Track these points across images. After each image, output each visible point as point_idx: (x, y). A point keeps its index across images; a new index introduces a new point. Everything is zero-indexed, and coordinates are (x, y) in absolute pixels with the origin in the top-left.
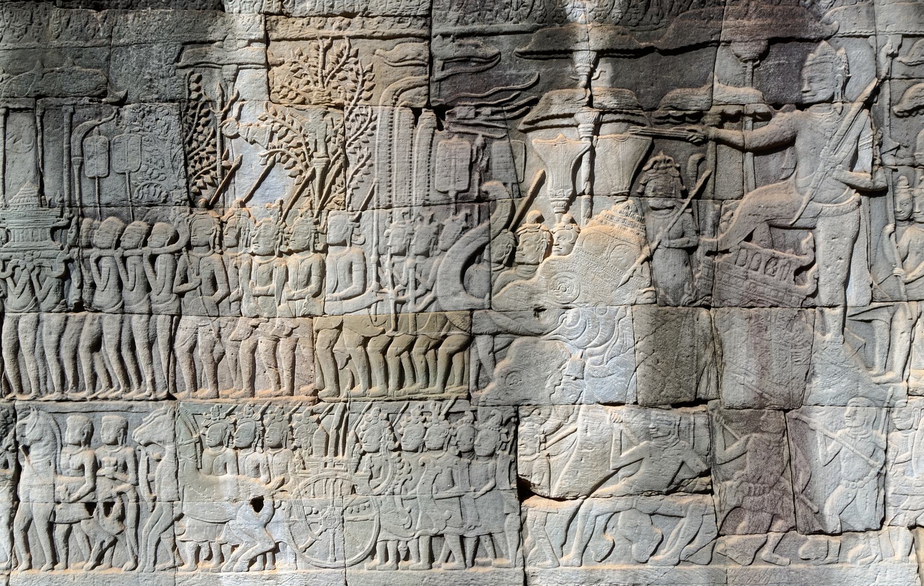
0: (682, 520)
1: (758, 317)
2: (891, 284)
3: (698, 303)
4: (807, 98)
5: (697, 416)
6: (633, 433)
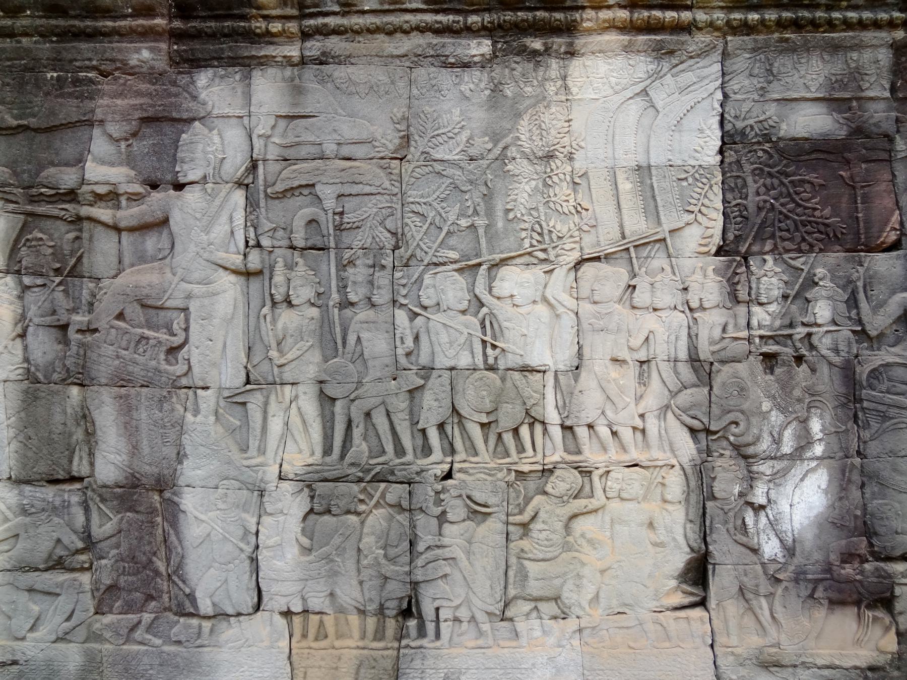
0: (60, 598)
1: (127, 396)
2: (265, 367)
3: (69, 381)
4: (182, 180)
5: (71, 494)
6: (9, 508)
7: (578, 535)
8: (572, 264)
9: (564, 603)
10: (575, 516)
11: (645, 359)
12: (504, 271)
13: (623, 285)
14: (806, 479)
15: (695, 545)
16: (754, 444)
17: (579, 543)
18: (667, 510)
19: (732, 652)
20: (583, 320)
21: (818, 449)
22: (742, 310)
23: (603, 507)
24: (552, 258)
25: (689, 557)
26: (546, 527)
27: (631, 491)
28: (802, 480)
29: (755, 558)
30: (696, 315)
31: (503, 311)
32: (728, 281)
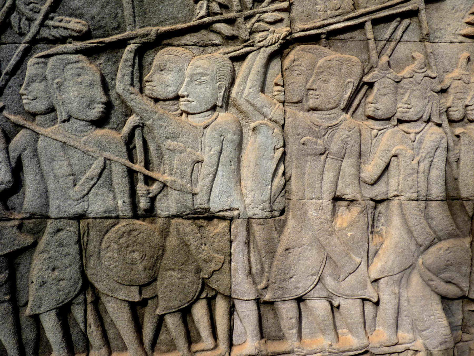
8: (275, 47)
11: (384, 197)
12: (162, 56)
13: (353, 81)
24: (244, 34)
31: (164, 122)
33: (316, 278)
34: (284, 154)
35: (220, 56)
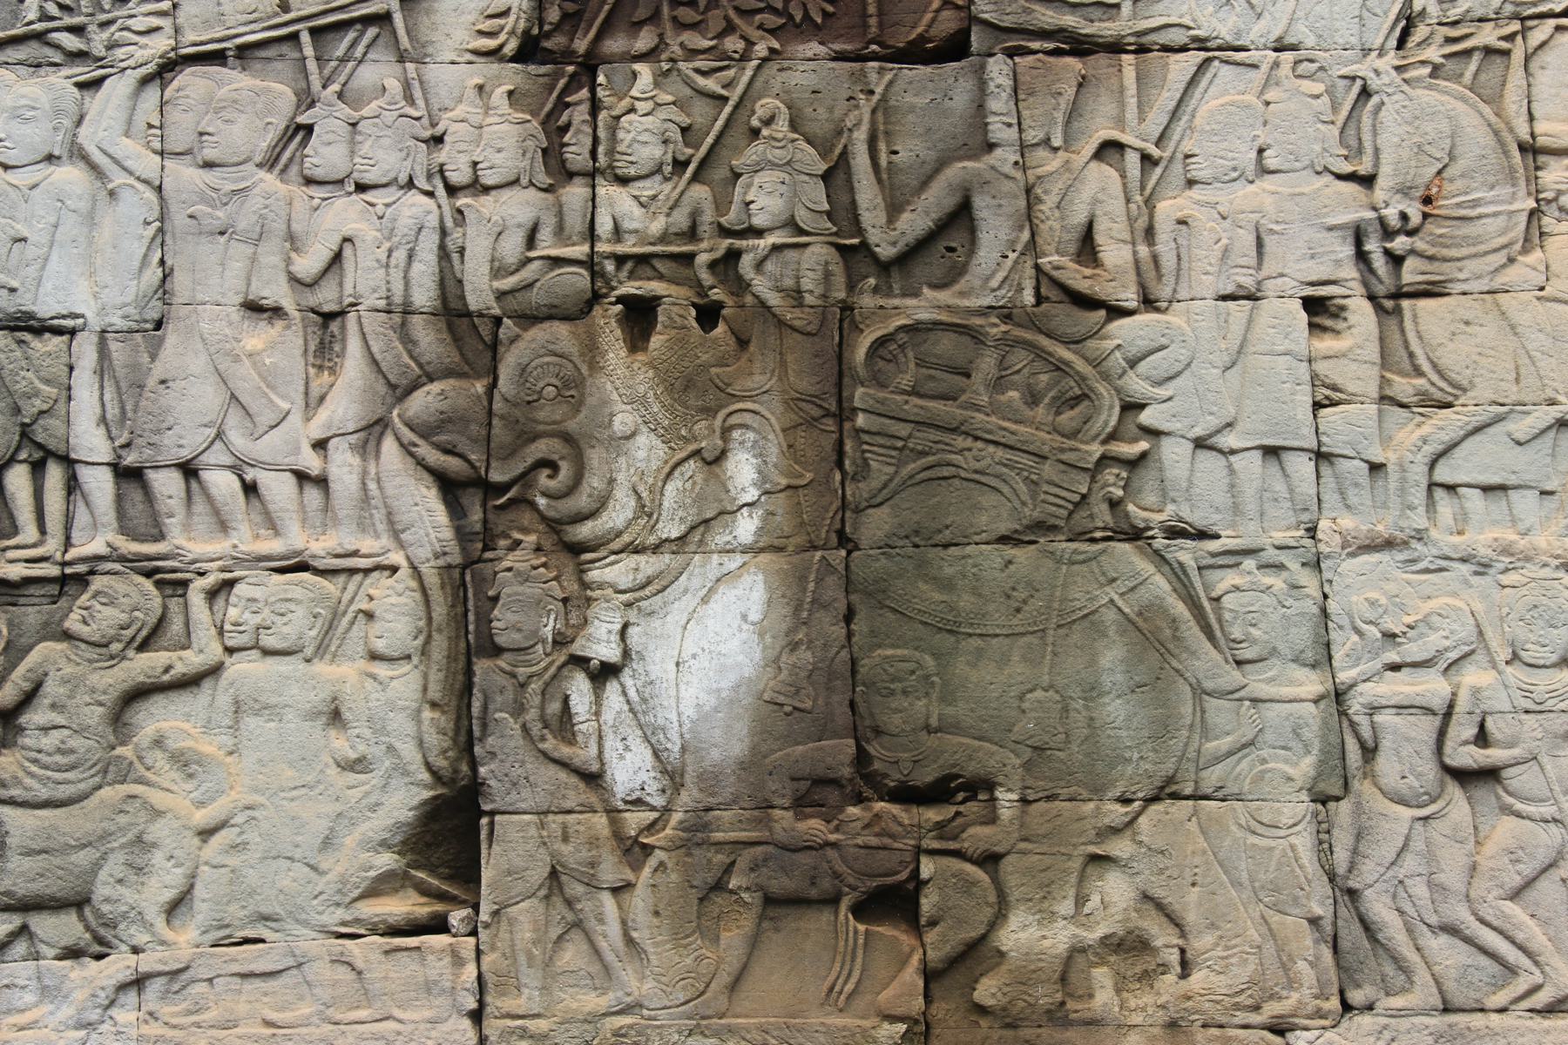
7: (145, 743)
8: (150, 68)
9: (98, 914)
10: (138, 694)
13: (279, 123)
14: (716, 597)
15: (441, 763)
16: (592, 514)
17: (149, 762)
18: (374, 677)
19: (524, 1029)
20: (173, 207)
21: (746, 527)
22: (575, 193)
23: (215, 671)
24: (98, 49)
25: (427, 794)
26: (60, 719)
27: (286, 630)
28: (705, 600)
29: (593, 799)
30: (462, 201)
32: (543, 123)
33: (212, 432)
34: (161, 230)
35: (61, 82)
